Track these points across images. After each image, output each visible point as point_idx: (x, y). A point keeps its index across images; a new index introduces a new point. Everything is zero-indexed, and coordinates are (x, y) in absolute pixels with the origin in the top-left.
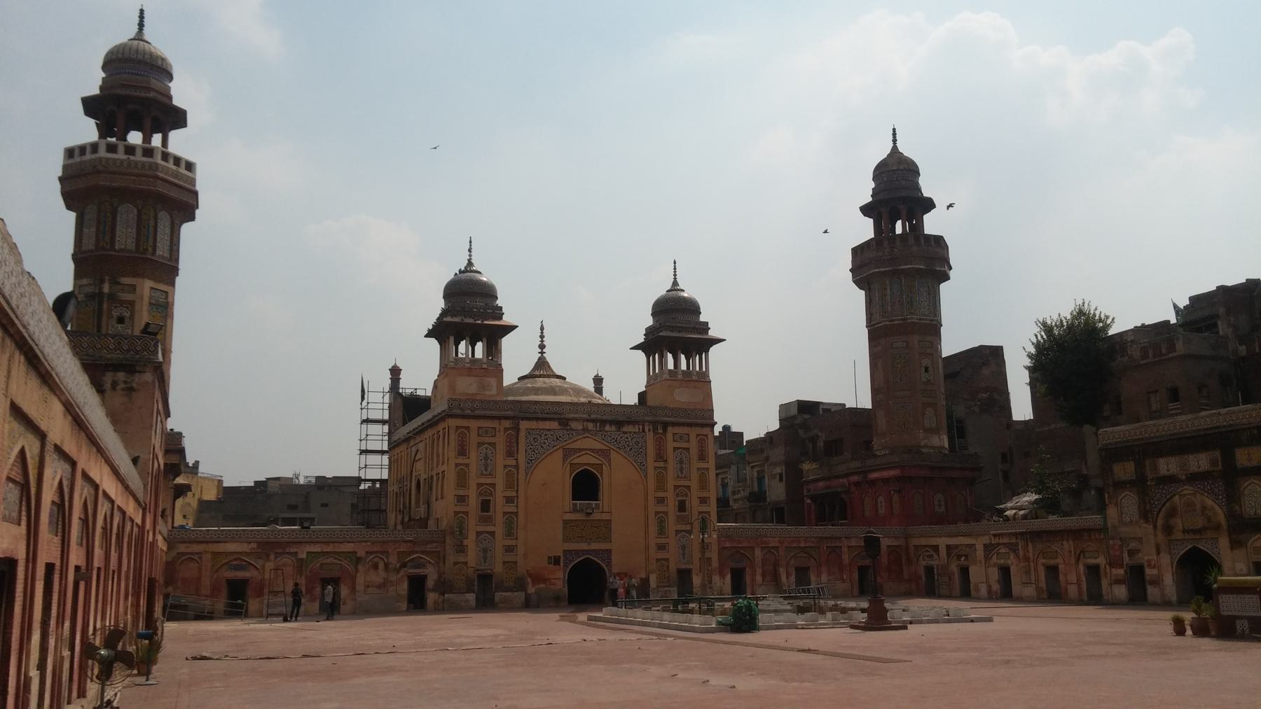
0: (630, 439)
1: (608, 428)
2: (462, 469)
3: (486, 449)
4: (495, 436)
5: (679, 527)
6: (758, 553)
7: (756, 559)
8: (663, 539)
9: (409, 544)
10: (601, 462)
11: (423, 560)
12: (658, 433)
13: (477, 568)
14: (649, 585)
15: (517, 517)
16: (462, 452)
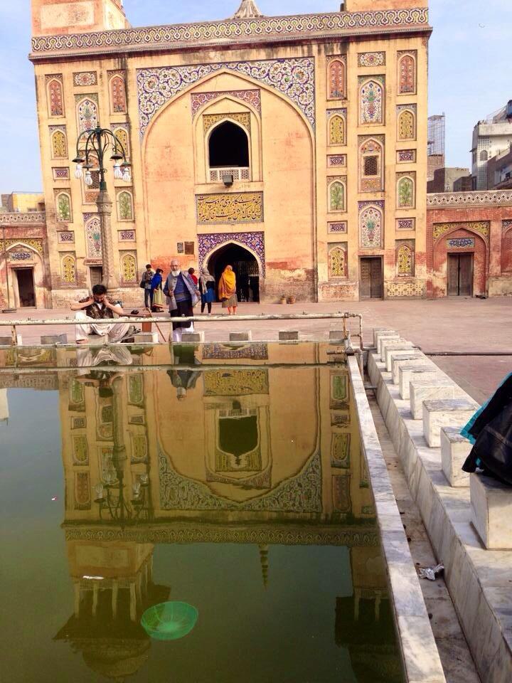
0: (289, 70)
1: (254, 54)
2: (59, 133)
3: (87, 103)
4: (96, 83)
5: (364, 197)
6: (496, 228)
7: (492, 239)
8: (339, 215)
9: (6, 231)
10: (248, 110)
11: (23, 249)
12: (333, 56)
13: (90, 259)
14: (317, 279)
15: (133, 194)
16: (57, 110)
